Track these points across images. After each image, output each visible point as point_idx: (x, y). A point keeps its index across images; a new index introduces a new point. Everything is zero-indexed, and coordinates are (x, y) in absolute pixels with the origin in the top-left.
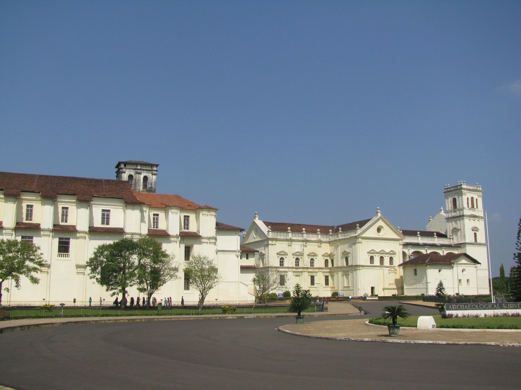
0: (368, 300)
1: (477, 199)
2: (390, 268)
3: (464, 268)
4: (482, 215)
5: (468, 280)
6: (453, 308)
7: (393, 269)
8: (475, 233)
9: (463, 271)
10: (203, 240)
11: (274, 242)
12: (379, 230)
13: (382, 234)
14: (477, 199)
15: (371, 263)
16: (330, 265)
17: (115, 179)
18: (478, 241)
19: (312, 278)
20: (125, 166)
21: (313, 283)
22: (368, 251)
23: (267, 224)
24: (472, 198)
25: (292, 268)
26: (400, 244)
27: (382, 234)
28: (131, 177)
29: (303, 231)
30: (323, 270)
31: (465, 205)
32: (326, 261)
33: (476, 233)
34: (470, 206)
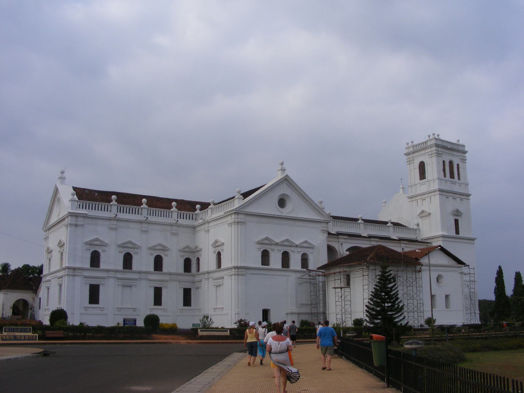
0: (202, 338)
1: (458, 165)
3: (440, 273)
5: (447, 297)
9: (438, 281)
11: (80, 221)
12: (282, 203)
13: (285, 212)
14: (458, 165)
15: (262, 265)
22: (257, 240)
24: (451, 163)
27: (285, 212)
29: (142, 204)
30: (180, 278)
33: (458, 220)
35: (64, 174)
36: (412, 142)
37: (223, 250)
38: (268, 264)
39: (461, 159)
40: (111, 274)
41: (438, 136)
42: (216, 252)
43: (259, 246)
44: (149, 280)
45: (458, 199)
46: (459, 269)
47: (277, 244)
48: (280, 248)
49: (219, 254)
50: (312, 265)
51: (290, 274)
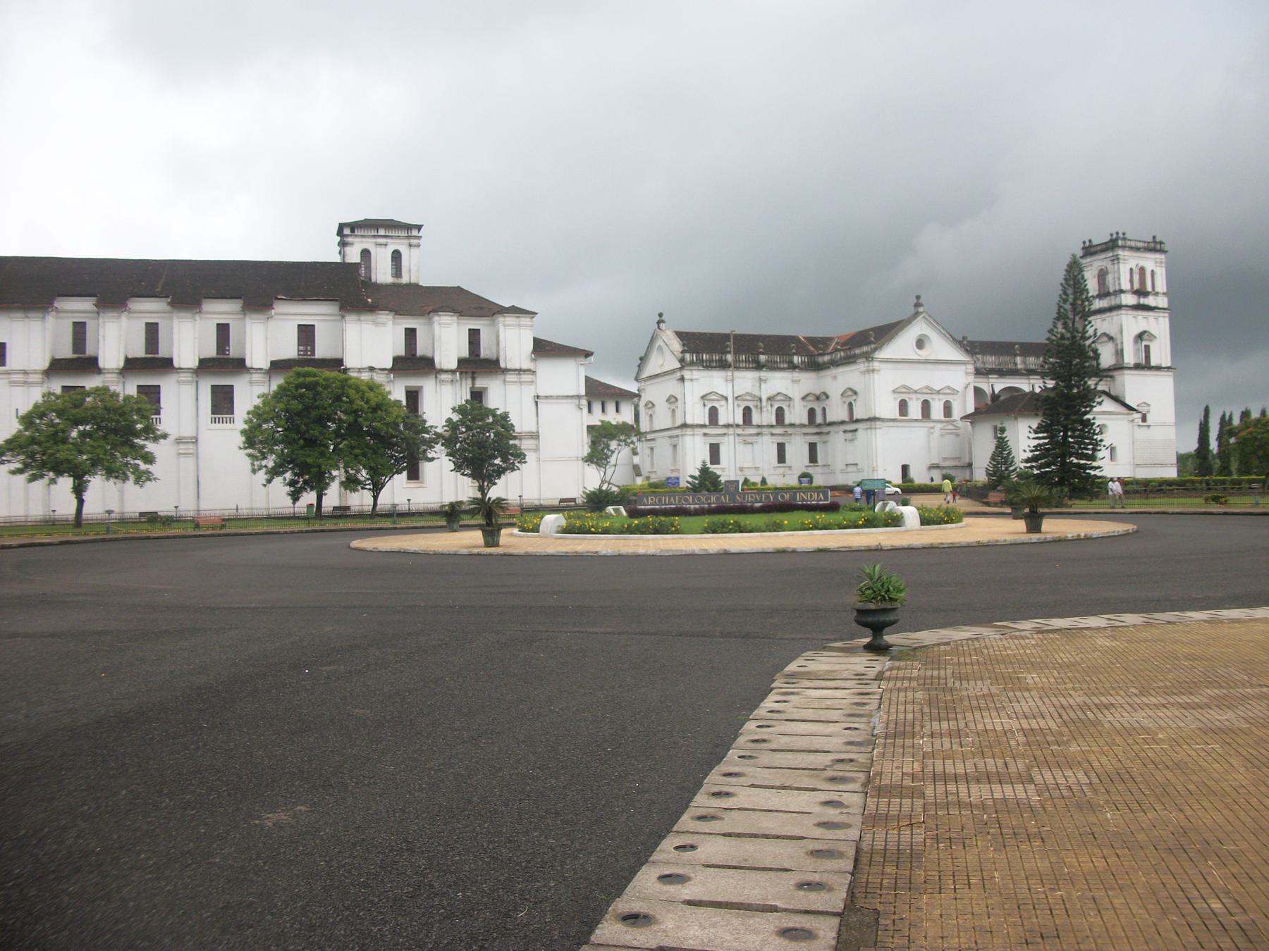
1: (1152, 271)
2: (944, 424)
4: (1162, 302)
6: (650, 501)
7: (951, 427)
8: (1145, 346)
10: (510, 377)
12: (920, 343)
13: (924, 354)
14: (1152, 271)
16: (819, 419)
17: (338, 259)
18: (1153, 363)
19: (781, 449)
20: (353, 231)
21: (781, 458)
23: (680, 335)
24: (1142, 270)
25: (738, 426)
26: (967, 373)
27: (924, 354)
28: (366, 254)
31: (1125, 285)
32: (812, 412)
34: (1136, 286)
35: (663, 318)
36: (1090, 241)
37: (855, 400)
38: (906, 415)
39: (1156, 262)
40: (731, 431)
41: (1124, 234)
42: (847, 403)
43: (896, 395)
44: (772, 434)
45: (1151, 319)
46: (1130, 416)
47: (916, 392)
48: (919, 396)
49: (850, 405)
50: (957, 413)
51: (931, 425)
